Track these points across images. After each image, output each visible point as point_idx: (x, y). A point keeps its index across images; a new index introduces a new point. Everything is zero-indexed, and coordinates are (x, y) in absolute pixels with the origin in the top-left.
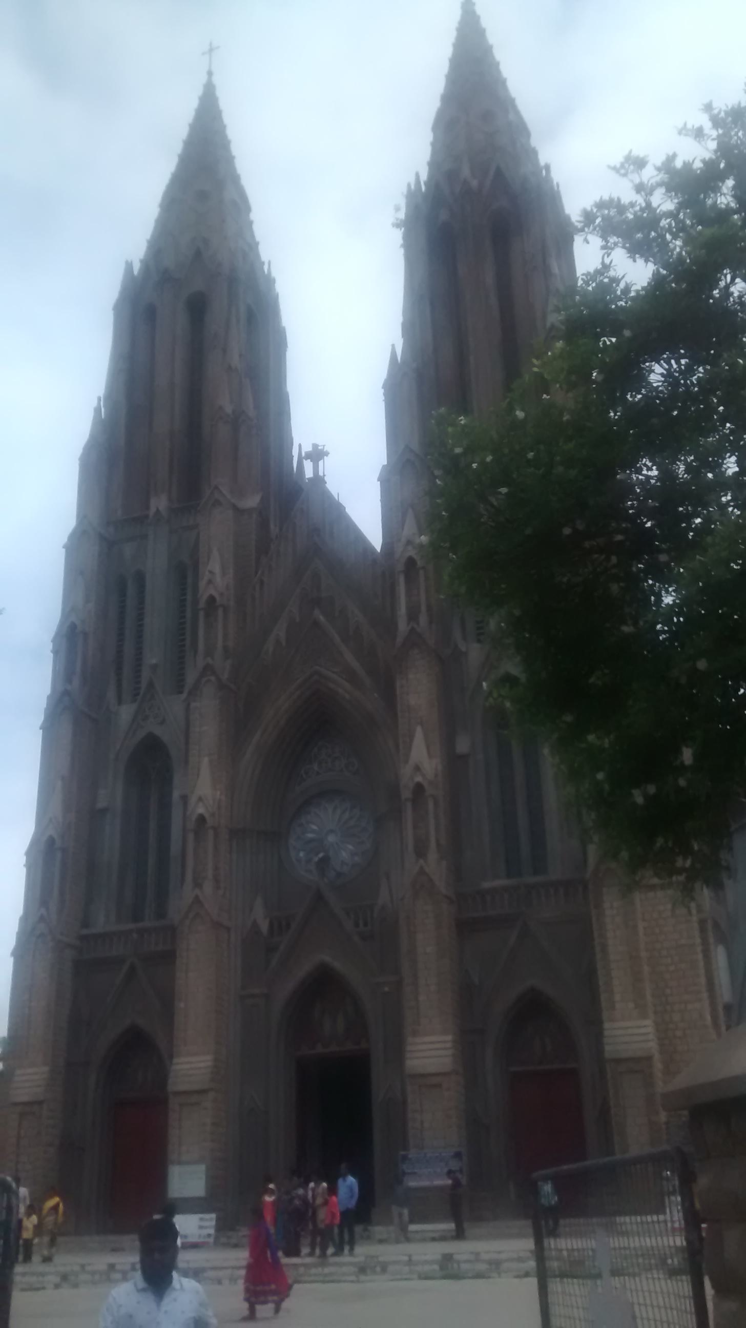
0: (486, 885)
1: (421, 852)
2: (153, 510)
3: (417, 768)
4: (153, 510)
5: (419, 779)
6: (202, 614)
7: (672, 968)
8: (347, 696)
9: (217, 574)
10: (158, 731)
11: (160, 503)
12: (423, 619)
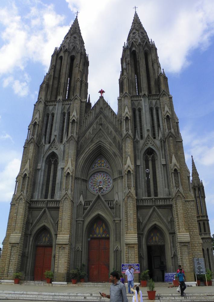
0: (144, 198)
1: (129, 187)
3: (129, 166)
4: (58, 99)
5: (129, 169)
6: (70, 124)
7: (190, 221)
8: (109, 148)
9: (75, 115)
10: (55, 151)
12: (130, 132)
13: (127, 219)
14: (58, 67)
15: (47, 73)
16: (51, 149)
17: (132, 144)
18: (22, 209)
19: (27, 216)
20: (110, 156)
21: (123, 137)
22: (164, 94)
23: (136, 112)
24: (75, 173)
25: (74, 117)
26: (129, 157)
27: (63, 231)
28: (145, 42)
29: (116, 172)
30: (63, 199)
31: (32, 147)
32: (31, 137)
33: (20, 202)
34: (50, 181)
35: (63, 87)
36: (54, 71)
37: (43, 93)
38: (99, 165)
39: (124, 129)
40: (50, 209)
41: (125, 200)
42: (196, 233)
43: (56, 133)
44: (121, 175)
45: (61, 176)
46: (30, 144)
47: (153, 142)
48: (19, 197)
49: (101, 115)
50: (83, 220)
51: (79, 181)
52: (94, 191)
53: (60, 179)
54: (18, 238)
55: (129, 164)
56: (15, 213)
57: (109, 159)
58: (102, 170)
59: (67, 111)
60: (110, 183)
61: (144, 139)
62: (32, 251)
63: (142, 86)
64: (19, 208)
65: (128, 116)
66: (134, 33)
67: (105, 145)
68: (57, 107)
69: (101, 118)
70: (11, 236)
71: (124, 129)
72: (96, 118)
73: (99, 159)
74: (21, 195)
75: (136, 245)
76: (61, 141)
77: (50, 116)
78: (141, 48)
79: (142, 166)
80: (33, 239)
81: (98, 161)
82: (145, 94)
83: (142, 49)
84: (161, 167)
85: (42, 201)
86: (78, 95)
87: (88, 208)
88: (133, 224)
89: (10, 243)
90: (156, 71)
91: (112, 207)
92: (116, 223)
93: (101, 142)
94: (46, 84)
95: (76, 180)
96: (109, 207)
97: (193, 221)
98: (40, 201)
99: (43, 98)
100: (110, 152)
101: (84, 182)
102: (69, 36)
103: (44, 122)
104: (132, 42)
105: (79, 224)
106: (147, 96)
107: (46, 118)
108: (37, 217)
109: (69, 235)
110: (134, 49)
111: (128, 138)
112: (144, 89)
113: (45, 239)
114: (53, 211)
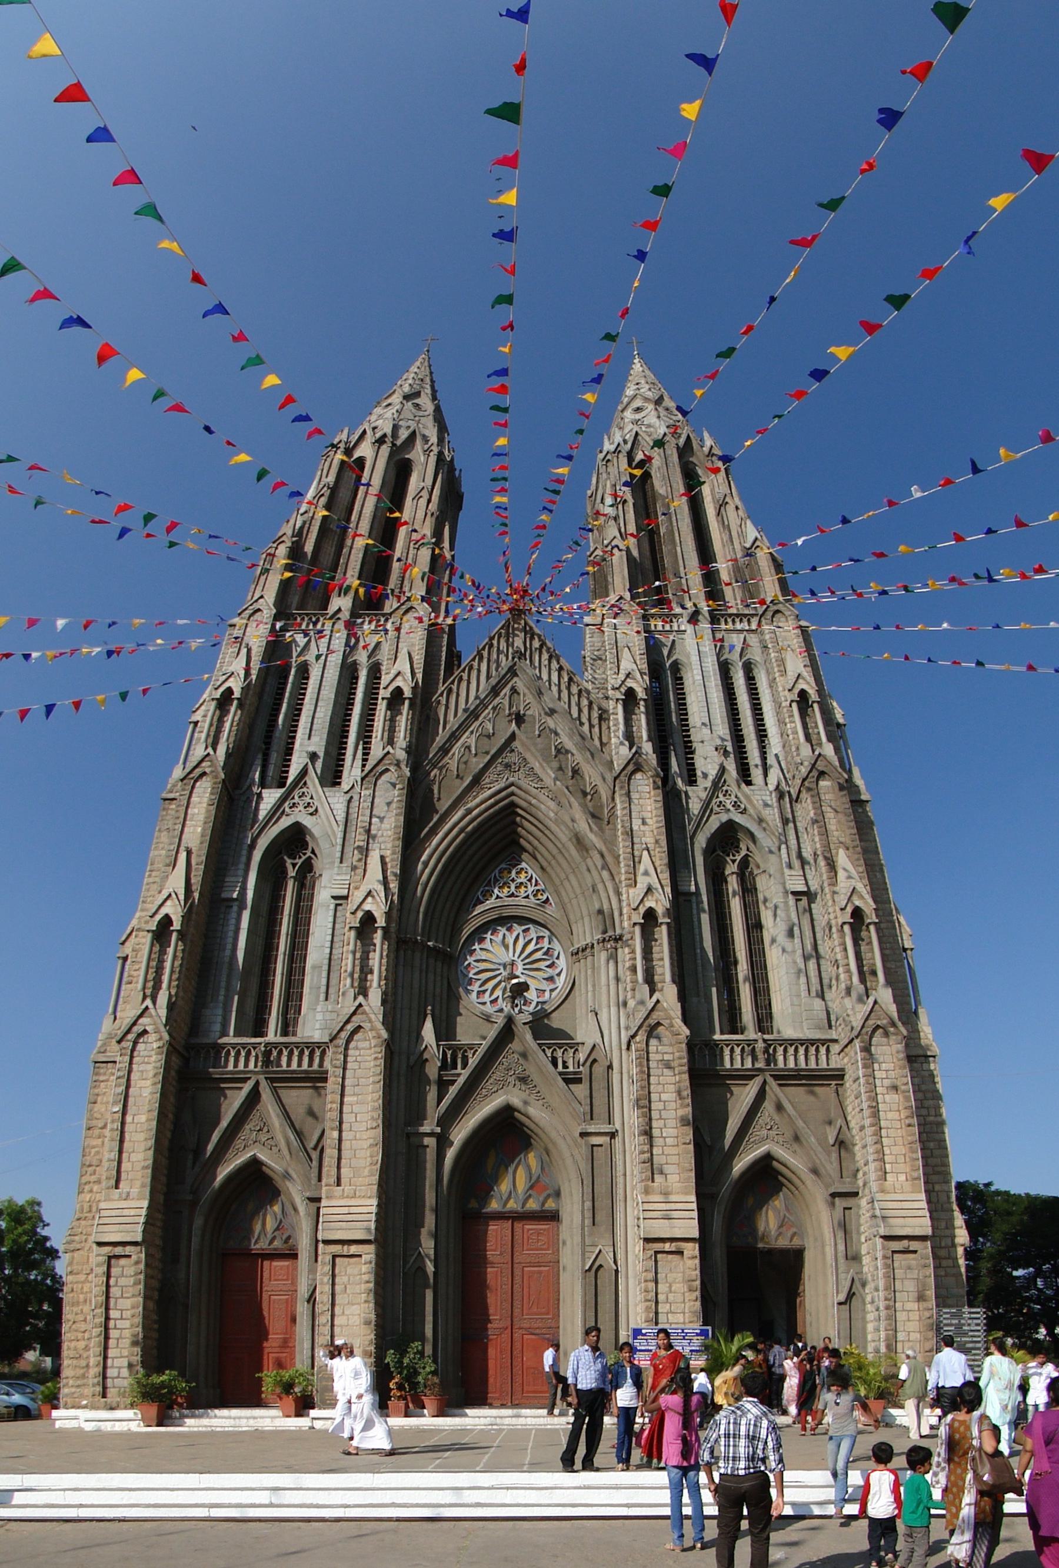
5: (650, 903)
6: (382, 707)
8: (552, 815)
10: (307, 821)
12: (647, 747)
13: (651, 1128)
16: (287, 810)
17: (660, 798)
20: (561, 852)
21: (617, 768)
23: (663, 673)
24: (400, 918)
26: (645, 853)
29: (586, 920)
32: (199, 751)
38: (506, 890)
41: (638, 1038)
43: (309, 741)
44: (610, 933)
45: (330, 932)
46: (196, 781)
47: (747, 797)
49: (515, 679)
50: (438, 1130)
51: (418, 955)
52: (484, 1004)
53: (328, 944)
55: (648, 886)
57: (553, 862)
58: (519, 912)
60: (557, 971)
61: (704, 784)
65: (634, 685)
67: (534, 801)
69: (514, 691)
73: (503, 866)
76: (332, 777)
79: (705, 898)
81: (500, 872)
84: (786, 903)
87: (459, 1075)
88: (675, 1151)
91: (575, 1073)
92: (593, 1146)
93: (520, 788)
95: (402, 952)
96: (560, 1074)
100: (560, 835)
101: (439, 964)
109: (374, 1202)
111: (639, 776)
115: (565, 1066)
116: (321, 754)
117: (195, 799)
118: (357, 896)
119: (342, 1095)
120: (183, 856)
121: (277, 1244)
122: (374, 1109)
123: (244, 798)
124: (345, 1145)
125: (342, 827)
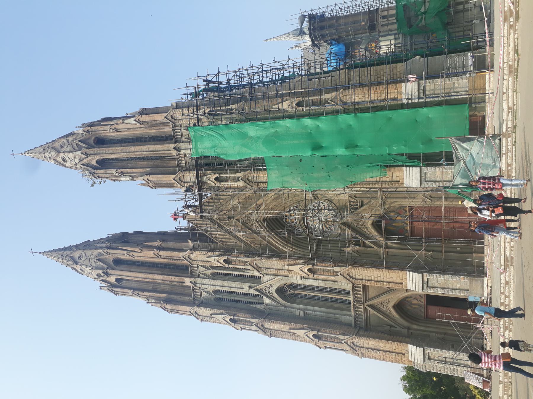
2: (191, 285)
4: (191, 285)
10: (275, 288)
11: (188, 281)
14: (134, 285)
15: (147, 303)
18: (370, 342)
19: (380, 334)
21: (248, 186)
22: (172, 117)
25: (220, 261)
27: (401, 281)
28: (80, 143)
30: (351, 280)
31: (271, 325)
32: (254, 328)
33: (358, 344)
34: (322, 295)
35: (169, 277)
36: (143, 290)
37: (181, 308)
39: (236, 184)
40: (366, 298)
42: (402, 68)
43: (245, 288)
48: (350, 346)
53: (318, 281)
54: (415, 349)
56: (376, 353)
59: (209, 269)
62: (435, 326)
63: (161, 152)
64: (368, 346)
66: (64, 159)
68: (203, 287)
69: (219, 219)
70: (413, 360)
71: (236, 184)
72: (219, 226)
74: (347, 344)
75: (423, 169)
76: (257, 280)
77: (218, 296)
78: (92, 152)
80: (416, 324)
82: (174, 148)
83: (93, 149)
85: (354, 309)
86: (181, 254)
89: (424, 361)
90: (131, 127)
94: (165, 304)
97: (382, 73)
98: (355, 312)
99: (188, 308)
102: (78, 267)
103: (229, 305)
104: (82, 165)
105: (389, 254)
106: (176, 144)
107: (223, 303)
108: (380, 317)
109: (408, 272)
110: (94, 163)
111: (250, 178)
112: (166, 149)
113: (414, 304)
114: (370, 293)
115: (357, 205)
116: (249, 284)
117: (272, 328)
118: (301, 273)
119: (372, 281)
120: (292, 331)
121: (422, 300)
122: (376, 271)
123: (268, 310)
124: (388, 280)
125: (276, 277)
